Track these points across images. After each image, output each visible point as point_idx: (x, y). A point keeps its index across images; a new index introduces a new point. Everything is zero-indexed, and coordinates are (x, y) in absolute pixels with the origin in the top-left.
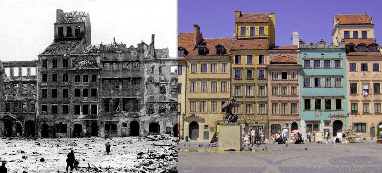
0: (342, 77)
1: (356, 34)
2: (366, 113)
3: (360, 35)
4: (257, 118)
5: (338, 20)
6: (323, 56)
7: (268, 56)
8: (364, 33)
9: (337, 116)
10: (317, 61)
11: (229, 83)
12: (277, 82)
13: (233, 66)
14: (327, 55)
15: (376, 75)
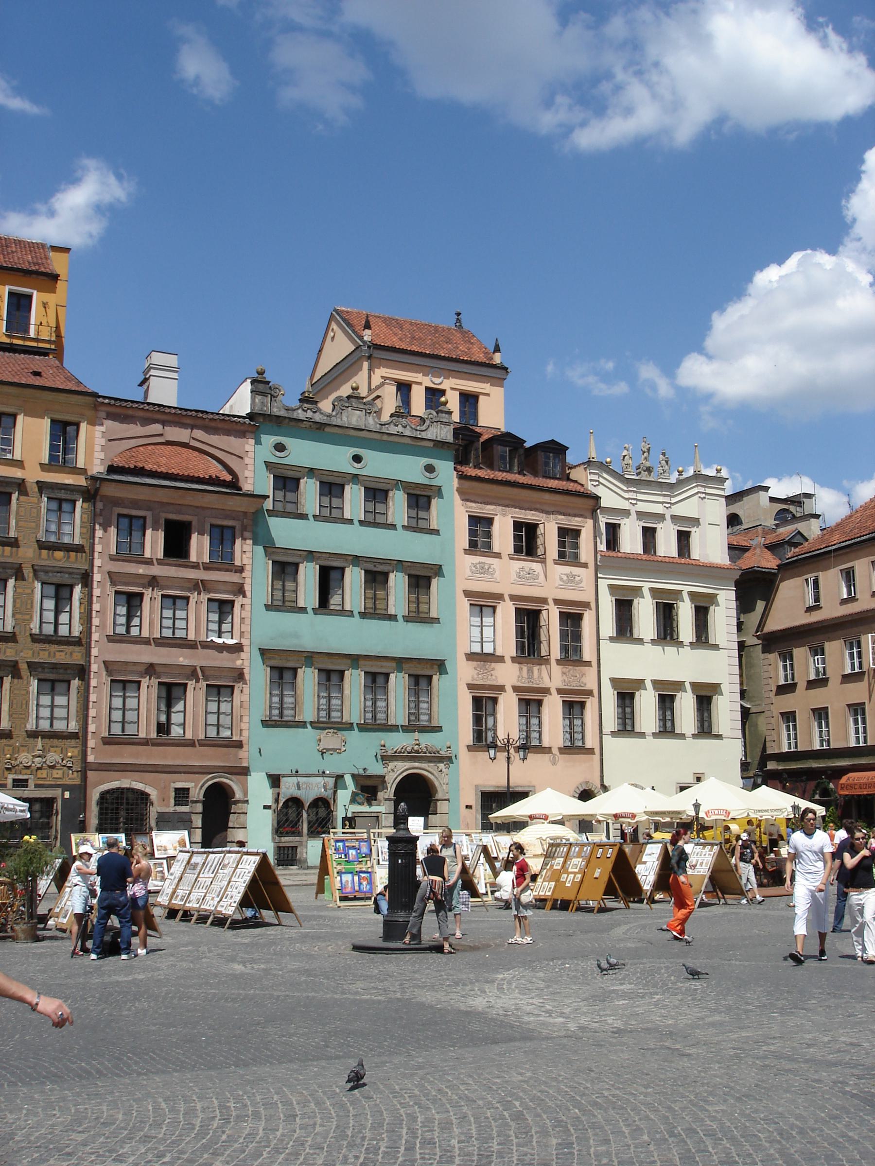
0: (438, 570)
1: (434, 395)
4: (25, 758)
5: (367, 326)
7: (99, 429)
8: (469, 400)
9: (413, 756)
10: (332, 487)
12: (141, 570)
14: (381, 465)
15: (571, 578)
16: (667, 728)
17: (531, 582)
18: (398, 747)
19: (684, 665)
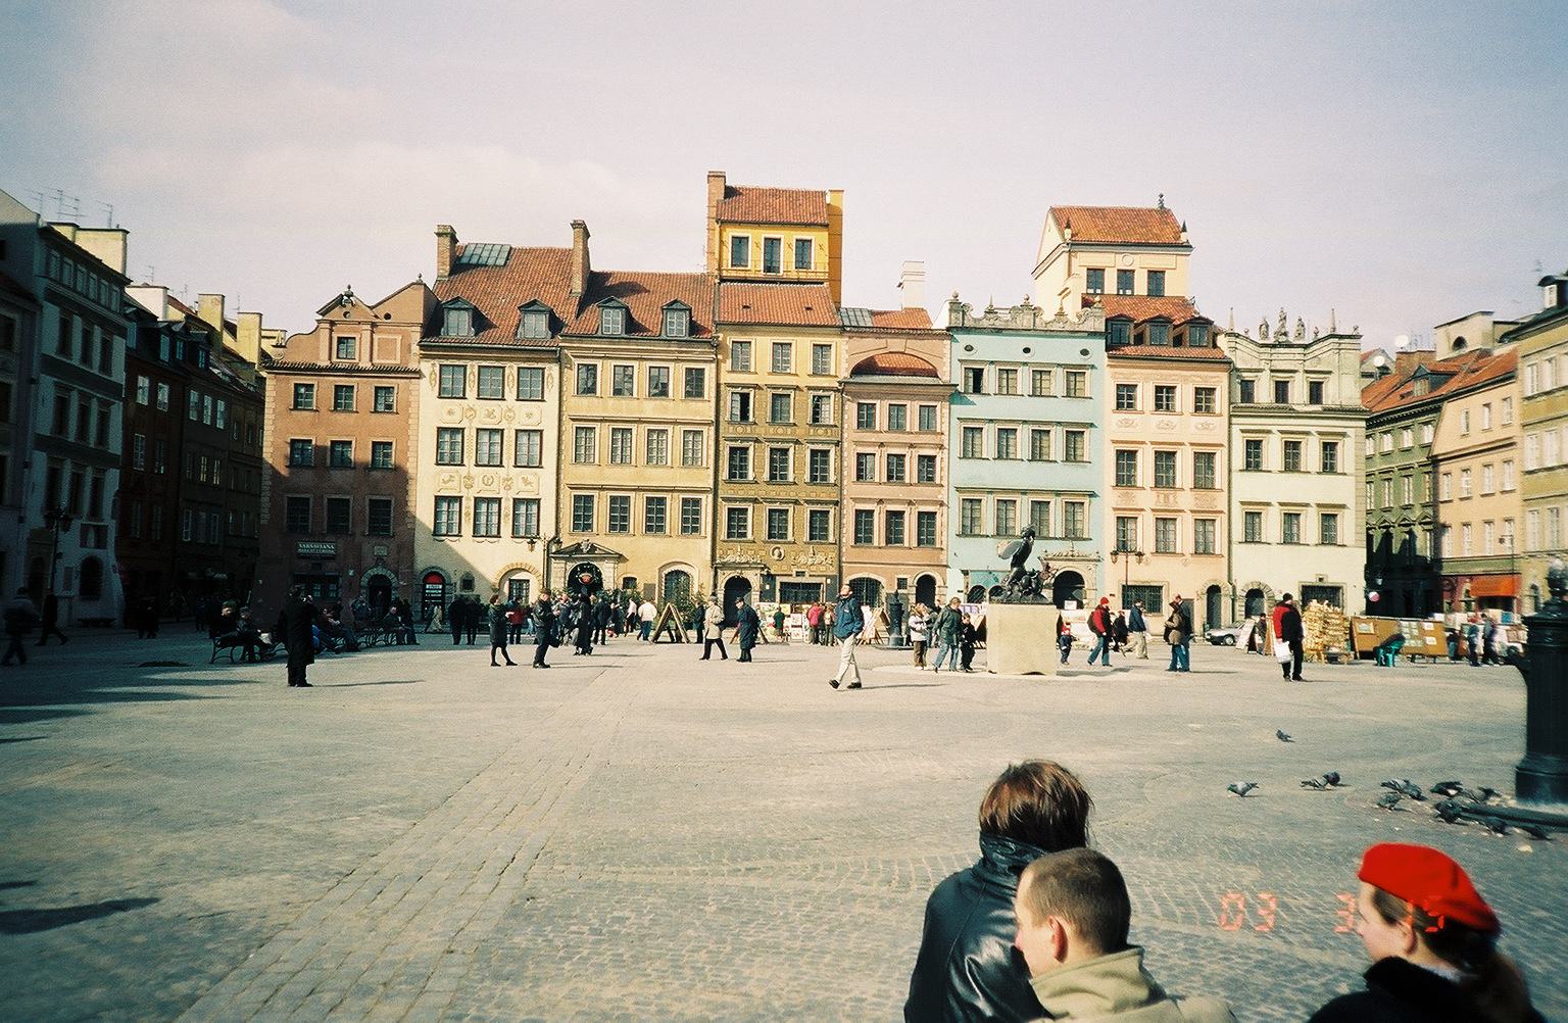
1: (1126, 277)
2: (1163, 548)
3: (1141, 286)
4: (802, 559)
5: (1068, 226)
6: (1026, 355)
8: (1156, 277)
9: (1071, 558)
10: (1007, 372)
11: (709, 433)
13: (726, 378)
16: (1289, 539)
17: (1170, 431)
18: (1056, 552)
19: (1310, 488)
